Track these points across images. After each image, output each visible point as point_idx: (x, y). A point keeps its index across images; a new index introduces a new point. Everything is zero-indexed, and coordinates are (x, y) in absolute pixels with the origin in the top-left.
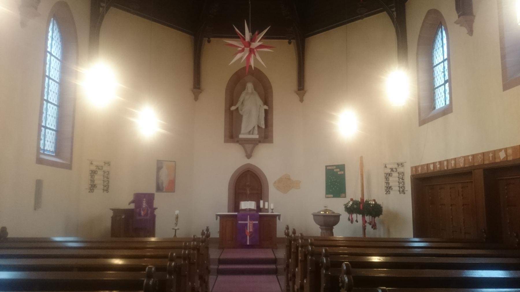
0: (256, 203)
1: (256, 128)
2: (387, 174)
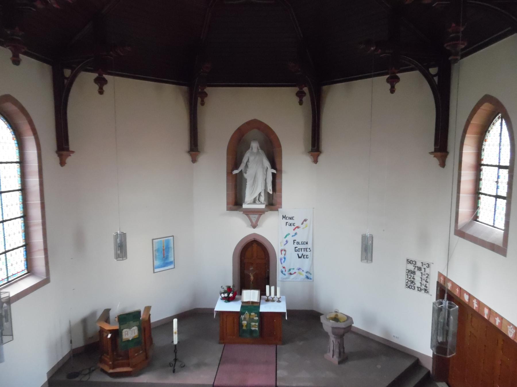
0: (260, 291)
1: (263, 194)
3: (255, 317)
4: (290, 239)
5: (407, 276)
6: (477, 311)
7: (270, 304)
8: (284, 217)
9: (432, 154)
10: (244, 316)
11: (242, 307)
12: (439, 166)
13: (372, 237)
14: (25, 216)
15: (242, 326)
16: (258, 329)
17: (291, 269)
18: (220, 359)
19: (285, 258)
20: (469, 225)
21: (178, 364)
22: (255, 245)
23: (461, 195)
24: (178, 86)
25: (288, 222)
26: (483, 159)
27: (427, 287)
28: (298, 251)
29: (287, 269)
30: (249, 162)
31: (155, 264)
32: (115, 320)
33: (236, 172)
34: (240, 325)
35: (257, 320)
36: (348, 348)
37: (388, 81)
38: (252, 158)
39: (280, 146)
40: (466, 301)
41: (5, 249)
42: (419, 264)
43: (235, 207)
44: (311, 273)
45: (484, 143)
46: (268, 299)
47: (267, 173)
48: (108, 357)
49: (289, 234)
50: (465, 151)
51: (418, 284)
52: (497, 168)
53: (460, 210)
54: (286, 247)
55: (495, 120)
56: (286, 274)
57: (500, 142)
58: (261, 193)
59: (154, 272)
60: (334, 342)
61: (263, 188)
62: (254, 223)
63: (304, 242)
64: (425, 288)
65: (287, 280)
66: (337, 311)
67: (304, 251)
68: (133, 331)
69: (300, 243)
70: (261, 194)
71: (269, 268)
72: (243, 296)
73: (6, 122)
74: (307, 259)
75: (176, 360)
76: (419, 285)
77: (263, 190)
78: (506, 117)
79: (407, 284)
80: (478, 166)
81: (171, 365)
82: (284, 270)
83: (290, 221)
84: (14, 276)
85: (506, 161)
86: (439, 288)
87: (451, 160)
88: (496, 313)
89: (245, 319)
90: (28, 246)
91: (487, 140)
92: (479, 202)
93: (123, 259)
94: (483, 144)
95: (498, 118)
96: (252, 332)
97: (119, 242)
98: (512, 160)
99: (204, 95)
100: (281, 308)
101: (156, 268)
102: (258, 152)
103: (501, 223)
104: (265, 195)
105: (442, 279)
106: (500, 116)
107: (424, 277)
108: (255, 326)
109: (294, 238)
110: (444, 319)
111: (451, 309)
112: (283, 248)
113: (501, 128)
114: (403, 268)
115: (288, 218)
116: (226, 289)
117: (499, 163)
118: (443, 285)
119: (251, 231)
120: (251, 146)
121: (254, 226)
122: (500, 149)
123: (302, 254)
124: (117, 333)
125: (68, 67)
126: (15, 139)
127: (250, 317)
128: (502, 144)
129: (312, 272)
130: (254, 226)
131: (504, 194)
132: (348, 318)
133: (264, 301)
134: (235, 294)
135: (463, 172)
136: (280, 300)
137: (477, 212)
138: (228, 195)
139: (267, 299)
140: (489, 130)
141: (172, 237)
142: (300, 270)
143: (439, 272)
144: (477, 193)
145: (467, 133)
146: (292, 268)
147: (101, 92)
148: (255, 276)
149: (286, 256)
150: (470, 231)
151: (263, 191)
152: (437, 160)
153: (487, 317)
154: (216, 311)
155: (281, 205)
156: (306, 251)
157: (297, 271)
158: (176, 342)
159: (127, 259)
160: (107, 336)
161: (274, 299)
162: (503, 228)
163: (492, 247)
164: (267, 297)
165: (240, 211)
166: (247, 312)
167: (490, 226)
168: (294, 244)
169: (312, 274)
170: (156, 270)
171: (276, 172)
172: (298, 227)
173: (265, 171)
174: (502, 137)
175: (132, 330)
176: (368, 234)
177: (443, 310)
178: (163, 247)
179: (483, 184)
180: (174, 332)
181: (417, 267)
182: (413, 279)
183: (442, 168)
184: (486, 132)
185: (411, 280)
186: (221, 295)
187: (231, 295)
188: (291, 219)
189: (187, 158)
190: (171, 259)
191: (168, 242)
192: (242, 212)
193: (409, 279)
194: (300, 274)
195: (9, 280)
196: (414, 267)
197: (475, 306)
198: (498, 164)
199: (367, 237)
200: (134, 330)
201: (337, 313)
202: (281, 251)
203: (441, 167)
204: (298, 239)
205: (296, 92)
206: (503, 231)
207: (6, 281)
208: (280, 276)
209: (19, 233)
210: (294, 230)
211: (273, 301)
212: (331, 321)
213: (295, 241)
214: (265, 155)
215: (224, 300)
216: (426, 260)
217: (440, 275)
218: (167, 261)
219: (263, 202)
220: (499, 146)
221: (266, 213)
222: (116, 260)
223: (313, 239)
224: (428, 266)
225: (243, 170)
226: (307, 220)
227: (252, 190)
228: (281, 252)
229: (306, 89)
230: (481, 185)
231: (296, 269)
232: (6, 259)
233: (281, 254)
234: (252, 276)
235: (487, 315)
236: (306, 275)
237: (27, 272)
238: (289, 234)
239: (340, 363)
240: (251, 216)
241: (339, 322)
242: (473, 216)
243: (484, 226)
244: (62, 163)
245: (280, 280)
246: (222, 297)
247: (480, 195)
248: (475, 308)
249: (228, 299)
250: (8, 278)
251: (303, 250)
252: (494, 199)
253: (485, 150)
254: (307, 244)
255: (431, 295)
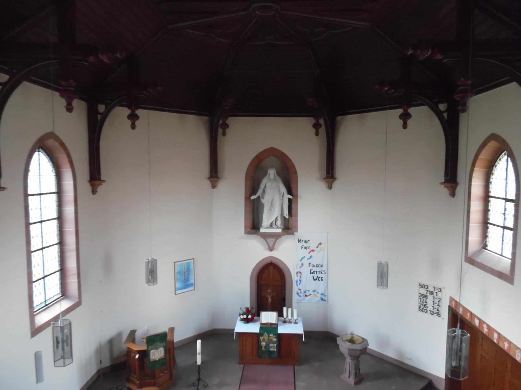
0: (277, 313)
1: (279, 219)
2: (422, 295)
3: (274, 338)
4: (306, 262)
5: (420, 299)
6: (487, 335)
7: (287, 325)
8: (300, 241)
9: (442, 185)
10: (263, 337)
11: (261, 328)
12: (449, 196)
13: (388, 265)
14: (61, 243)
15: (261, 347)
16: (276, 350)
17: (307, 291)
18: (240, 379)
19: (300, 281)
20: (478, 253)
21: (201, 383)
22: (271, 268)
23: (470, 224)
24: (200, 117)
25: (303, 246)
26: (490, 191)
27: (439, 311)
28: (314, 274)
29: (303, 292)
30: (266, 188)
31: (176, 286)
32: (143, 341)
33: (253, 197)
34: (259, 346)
35: (276, 341)
36: (364, 368)
37: (401, 117)
38: (268, 185)
39: (296, 173)
40: (476, 326)
41: (44, 274)
42: (431, 289)
43: (253, 231)
44: (325, 295)
45: (492, 177)
46: (285, 320)
47: (284, 198)
48: (135, 376)
49: (305, 257)
50: (473, 183)
51: (430, 308)
52: (504, 201)
53: (470, 239)
54: (302, 270)
55: (501, 156)
56: (301, 296)
57: (507, 176)
58: (278, 217)
59: (176, 294)
60: (350, 363)
61: (280, 213)
62: (271, 246)
63: (319, 265)
64: (438, 312)
65: (303, 302)
66: (353, 333)
67: (319, 273)
68: (160, 351)
69: (315, 266)
70: (278, 218)
71: (285, 290)
72: (261, 317)
73: (47, 156)
74: (322, 281)
75: (199, 379)
76: (431, 309)
77: (279, 215)
78: (511, 155)
79: (419, 308)
80: (486, 198)
81: (195, 385)
82: (299, 292)
83: (306, 245)
84: (50, 299)
85: (512, 195)
86: (450, 312)
87: (460, 190)
88: (505, 338)
89: (264, 340)
90: (63, 271)
91: (494, 174)
92: (487, 231)
93: (154, 284)
94: (491, 177)
95: (504, 154)
96: (270, 353)
97: (150, 268)
98: (517, 195)
99: (225, 126)
100: (298, 329)
101: (177, 290)
102: (275, 179)
103: (508, 252)
104: (281, 219)
105: (454, 303)
106: (506, 153)
107: (436, 301)
108: (273, 347)
109: (310, 261)
110: (457, 346)
111: (464, 337)
112: (298, 270)
113: (507, 164)
114: (415, 292)
115: (303, 242)
116: (245, 311)
117: (506, 196)
118: (455, 309)
119: (268, 254)
120: (268, 173)
121: (271, 249)
122: (506, 183)
123: (317, 277)
124: (144, 354)
125: (102, 103)
126: (54, 171)
127: (268, 338)
128: (508, 179)
129: (326, 294)
130: (271, 249)
131: (511, 226)
132: (364, 339)
133: (282, 322)
134: (253, 317)
135: (472, 203)
136: (297, 321)
137: (485, 242)
138: (246, 219)
139: (284, 321)
140: (496, 164)
141: (193, 260)
142: (315, 292)
143: (450, 297)
144: (485, 223)
145: (475, 167)
146: (307, 290)
147: (133, 127)
148: (273, 298)
149: (301, 279)
150: (480, 259)
151: (280, 216)
152: (447, 190)
153: (497, 342)
154: (235, 332)
155: (297, 228)
156: (321, 274)
157: (312, 293)
158: (199, 362)
159: (157, 284)
160: (135, 356)
161: (291, 320)
162: (510, 257)
163: (500, 275)
164: (284, 319)
165: (258, 235)
166: (265, 334)
167: (498, 254)
168: (309, 267)
169: (327, 296)
170: (177, 292)
171: (293, 197)
172: (313, 251)
173: (282, 196)
174: (508, 173)
175: (159, 351)
176: (383, 262)
177: (457, 338)
178: (185, 269)
179: (490, 242)
180: (198, 353)
181: (430, 291)
182: (425, 302)
183: (452, 198)
184: (493, 166)
185: (423, 304)
186: (240, 317)
187: (250, 316)
188: (307, 243)
189: (207, 184)
190: (192, 281)
191: (189, 265)
192: (259, 236)
193: (422, 303)
194: (315, 296)
195: (47, 303)
196: (426, 292)
197: (485, 330)
198: (505, 197)
199: (382, 265)
200: (161, 351)
201: (353, 335)
202: (297, 273)
203: (451, 196)
204: (313, 261)
205: (313, 124)
206: (510, 261)
207: (44, 305)
208: (295, 298)
209: (56, 258)
210: (309, 253)
211: (290, 322)
212: (347, 343)
213: (310, 264)
214: (281, 181)
215: (244, 322)
216: (438, 285)
217: (452, 299)
218: (187, 284)
219: (279, 226)
220: (505, 180)
221: (283, 237)
222: (147, 285)
223: (327, 263)
224: (440, 290)
225: (260, 196)
226: (322, 243)
227: (270, 214)
228: (297, 275)
229: (322, 121)
230: (489, 215)
231: (311, 291)
232: (44, 284)
233: (297, 276)
234: (270, 298)
235: (497, 340)
236: (321, 297)
237: (61, 295)
238: (305, 257)
239: (356, 383)
240: (268, 240)
241: (355, 344)
242: (482, 245)
243: (491, 254)
244: (94, 192)
245: (296, 302)
246: (241, 318)
247: (489, 225)
248: (485, 333)
249: (247, 321)
250: (45, 301)
251: (318, 272)
252: (502, 229)
253: (492, 183)
254: (322, 267)
255: (443, 319)
